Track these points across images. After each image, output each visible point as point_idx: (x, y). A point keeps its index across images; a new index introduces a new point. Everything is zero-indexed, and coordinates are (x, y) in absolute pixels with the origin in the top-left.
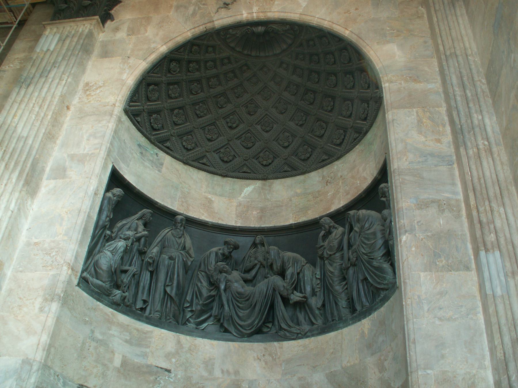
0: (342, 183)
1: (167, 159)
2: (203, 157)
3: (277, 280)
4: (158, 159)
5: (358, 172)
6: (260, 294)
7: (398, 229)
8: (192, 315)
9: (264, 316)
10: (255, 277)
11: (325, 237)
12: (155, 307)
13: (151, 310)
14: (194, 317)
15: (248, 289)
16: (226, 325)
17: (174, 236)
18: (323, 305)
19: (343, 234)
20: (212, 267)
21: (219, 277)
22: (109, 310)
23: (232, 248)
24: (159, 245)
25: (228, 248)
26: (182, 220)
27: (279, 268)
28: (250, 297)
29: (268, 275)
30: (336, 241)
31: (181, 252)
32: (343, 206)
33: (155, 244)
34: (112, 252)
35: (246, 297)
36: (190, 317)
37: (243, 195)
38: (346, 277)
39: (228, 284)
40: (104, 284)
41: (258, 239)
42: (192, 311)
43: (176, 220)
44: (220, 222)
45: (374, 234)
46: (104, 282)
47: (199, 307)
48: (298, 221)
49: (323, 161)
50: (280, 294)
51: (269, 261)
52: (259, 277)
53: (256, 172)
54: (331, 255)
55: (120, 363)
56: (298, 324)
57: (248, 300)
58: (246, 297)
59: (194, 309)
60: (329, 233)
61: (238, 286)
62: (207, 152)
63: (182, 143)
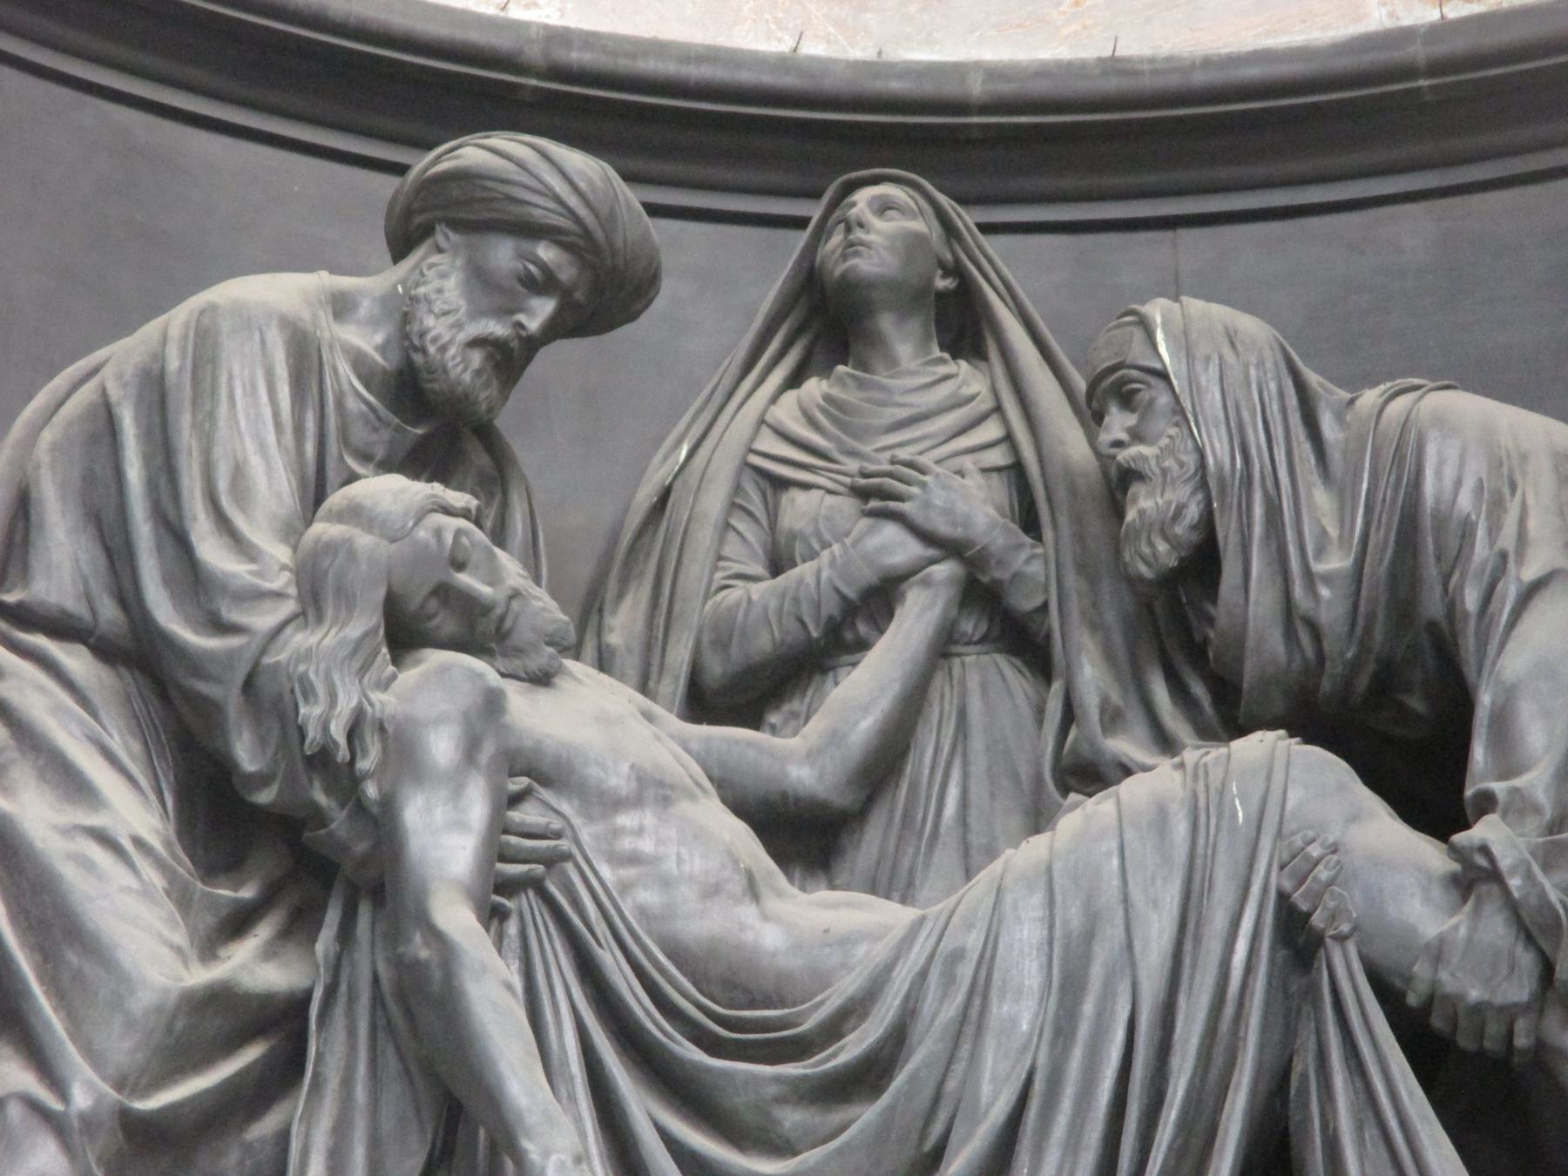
3: (1302, 787)
6: (1068, 987)
20: (254, 553)
21: (385, 702)
23: (543, 283)
25: (479, 277)
27: (1329, 606)
29: (1126, 745)
35: (834, 1030)
39: (528, 815)
51: (1144, 503)
52: (943, 783)
57: (868, 1077)
58: (834, 1030)
61: (680, 861)
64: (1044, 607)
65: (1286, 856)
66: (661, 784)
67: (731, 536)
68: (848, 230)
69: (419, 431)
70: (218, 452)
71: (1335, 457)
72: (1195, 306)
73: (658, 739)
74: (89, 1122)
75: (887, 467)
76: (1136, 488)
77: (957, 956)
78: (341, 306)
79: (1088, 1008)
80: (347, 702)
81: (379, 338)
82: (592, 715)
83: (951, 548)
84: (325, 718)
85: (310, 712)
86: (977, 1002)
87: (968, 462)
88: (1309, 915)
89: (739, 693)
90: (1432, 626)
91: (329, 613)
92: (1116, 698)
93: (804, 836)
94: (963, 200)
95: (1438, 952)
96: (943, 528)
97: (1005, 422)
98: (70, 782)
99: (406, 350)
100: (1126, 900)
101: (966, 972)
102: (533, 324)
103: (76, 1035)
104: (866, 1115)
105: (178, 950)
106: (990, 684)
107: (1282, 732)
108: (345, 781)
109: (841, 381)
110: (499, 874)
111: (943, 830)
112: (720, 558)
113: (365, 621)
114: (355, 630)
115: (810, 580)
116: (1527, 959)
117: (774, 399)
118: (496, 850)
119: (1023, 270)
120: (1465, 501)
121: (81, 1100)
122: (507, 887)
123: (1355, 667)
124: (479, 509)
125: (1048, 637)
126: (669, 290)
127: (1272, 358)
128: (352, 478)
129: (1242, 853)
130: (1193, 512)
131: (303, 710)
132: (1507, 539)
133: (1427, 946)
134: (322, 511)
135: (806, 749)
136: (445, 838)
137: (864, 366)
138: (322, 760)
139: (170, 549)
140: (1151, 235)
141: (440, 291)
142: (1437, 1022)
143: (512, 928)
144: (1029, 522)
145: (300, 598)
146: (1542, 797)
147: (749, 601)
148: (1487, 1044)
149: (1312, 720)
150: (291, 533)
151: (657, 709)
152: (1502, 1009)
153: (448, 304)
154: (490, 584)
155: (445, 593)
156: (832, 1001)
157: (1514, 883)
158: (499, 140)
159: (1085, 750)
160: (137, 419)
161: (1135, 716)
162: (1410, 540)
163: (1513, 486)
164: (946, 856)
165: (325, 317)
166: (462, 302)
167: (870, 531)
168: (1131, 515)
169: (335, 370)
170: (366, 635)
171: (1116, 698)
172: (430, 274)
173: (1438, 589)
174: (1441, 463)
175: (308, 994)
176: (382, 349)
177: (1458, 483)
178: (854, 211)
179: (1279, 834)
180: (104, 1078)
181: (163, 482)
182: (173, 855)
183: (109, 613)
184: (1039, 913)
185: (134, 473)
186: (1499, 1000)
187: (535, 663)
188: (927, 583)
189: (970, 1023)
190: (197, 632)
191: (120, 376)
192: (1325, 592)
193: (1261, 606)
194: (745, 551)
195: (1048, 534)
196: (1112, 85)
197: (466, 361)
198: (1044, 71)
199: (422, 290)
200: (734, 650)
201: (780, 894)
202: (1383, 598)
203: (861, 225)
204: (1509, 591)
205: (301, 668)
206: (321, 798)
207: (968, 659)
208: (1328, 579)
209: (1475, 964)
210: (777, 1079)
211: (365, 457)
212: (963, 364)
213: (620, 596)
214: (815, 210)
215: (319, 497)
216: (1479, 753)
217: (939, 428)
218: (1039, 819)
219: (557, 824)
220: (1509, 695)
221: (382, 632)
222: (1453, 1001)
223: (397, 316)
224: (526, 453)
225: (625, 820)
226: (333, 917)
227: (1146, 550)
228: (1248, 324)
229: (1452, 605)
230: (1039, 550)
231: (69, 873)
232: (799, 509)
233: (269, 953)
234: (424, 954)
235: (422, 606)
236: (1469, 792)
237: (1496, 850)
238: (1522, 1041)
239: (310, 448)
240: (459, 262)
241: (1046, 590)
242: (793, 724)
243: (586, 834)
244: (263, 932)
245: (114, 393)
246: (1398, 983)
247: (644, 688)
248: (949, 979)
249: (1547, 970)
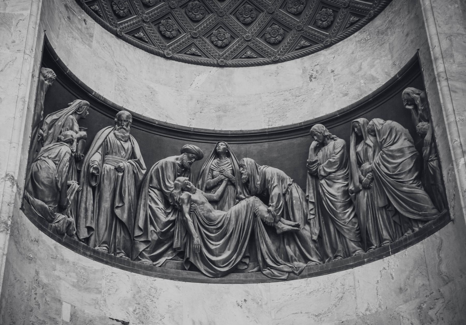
0: (335, 80)
1: (97, 29)
2: (138, 30)
4: (87, 28)
5: (360, 69)
7: (451, 148)
8: (147, 248)
9: (244, 250)
11: (317, 149)
12: (101, 236)
13: (95, 241)
14: (148, 249)
15: (217, 214)
16: (192, 260)
17: (119, 139)
18: (320, 237)
19: (347, 147)
20: (170, 183)
21: (181, 197)
22: (51, 242)
23: (194, 158)
24: (100, 151)
26: (128, 117)
27: (258, 186)
30: (338, 156)
31: (130, 161)
32: (338, 111)
33: (95, 148)
34: (54, 160)
36: (144, 250)
37: (194, 86)
38: (355, 203)
39: (193, 206)
40: (46, 206)
41: (222, 146)
42: (147, 242)
43: (120, 116)
44: (169, 121)
45: (401, 150)
46: (46, 203)
47: (155, 237)
48: (274, 126)
49: (302, 47)
50: (262, 221)
51: (244, 176)
53: (209, 55)
54: (330, 173)
55: (69, 316)
56: (287, 259)
59: (150, 239)
60: (322, 144)
62: (144, 21)
63: (112, 7)
72: (248, 159)
74: (159, 233)
80: (178, 196)
82: (199, 196)
83: (227, 177)
87: (229, 169)
89: (209, 189)
95: (266, 218)
98: (156, 203)
101: (228, 219)
102: (193, 161)
103: (157, 225)
106: (231, 189)
108: (178, 203)
116: (273, 219)
118: (190, 209)
119: (233, 148)
120: (269, 179)
122: (191, 211)
132: (273, 182)
135: (215, 195)
136: (186, 209)
138: (177, 201)
144: (234, 175)
150: (174, 181)
155: (187, 187)
162: (265, 181)
183: (159, 187)
185: (161, 176)
189: (229, 223)
193: (253, 186)
198: (235, 131)
204: (272, 187)
209: (270, 220)
216: (270, 201)
217: (227, 165)
220: (273, 196)
222: (267, 222)
225: (201, 206)
229: (268, 187)
231: (156, 211)
232: (215, 173)
244: (172, 214)
247: (202, 190)
249: (275, 220)
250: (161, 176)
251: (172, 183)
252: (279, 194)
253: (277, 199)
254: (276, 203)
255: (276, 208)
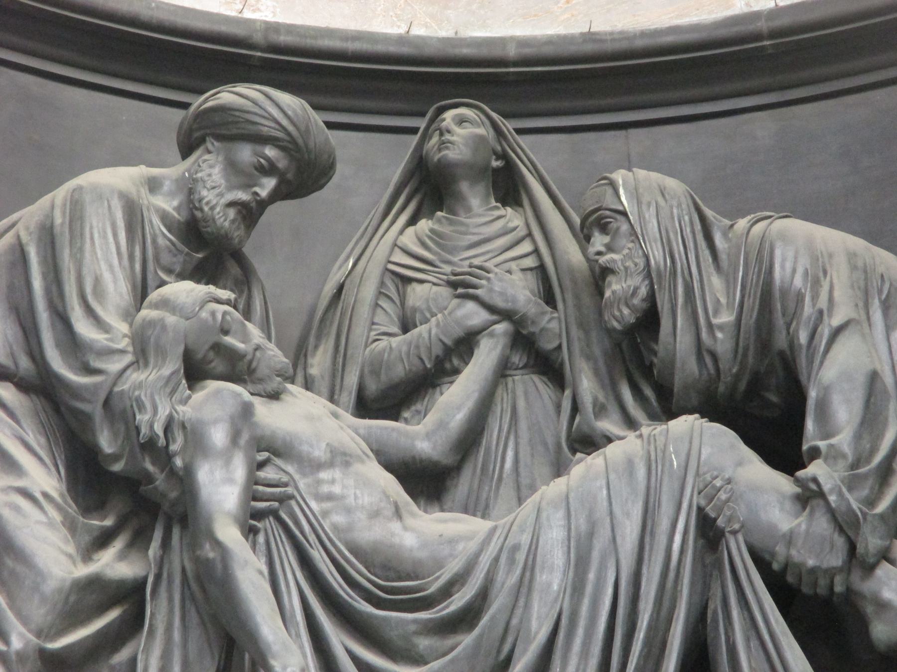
6: (580, 564)
10: (470, 440)
20: (107, 327)
21: (185, 411)
23: (268, 169)
25: (232, 166)
27: (722, 343)
28: (483, 596)
29: (608, 425)
35: (447, 592)
39: (269, 473)
50: (761, 562)
51: (615, 287)
52: (504, 449)
57: (466, 619)
58: (447, 592)
61: (356, 498)
64: (559, 347)
65: (701, 486)
66: (345, 454)
67: (379, 311)
68: (441, 134)
69: (200, 256)
70: (85, 271)
71: (723, 257)
72: (641, 173)
73: (342, 428)
74: (21, 656)
75: (469, 270)
76: (610, 278)
77: (516, 548)
78: (153, 185)
79: (591, 576)
80: (163, 412)
81: (175, 203)
82: (304, 416)
83: (506, 315)
84: (152, 420)
85: (142, 418)
86: (528, 574)
87: (513, 265)
88: (715, 520)
90: (781, 354)
91: (152, 360)
92: (601, 398)
93: (426, 481)
94: (506, 116)
95: (789, 539)
96: (500, 303)
97: (534, 241)
99: (191, 209)
100: (611, 513)
101: (521, 557)
102: (264, 193)
104: (467, 640)
105: (70, 556)
106: (529, 391)
107: (697, 415)
108: (164, 457)
109: (439, 221)
110: (253, 508)
111: (505, 476)
112: (373, 324)
113: (173, 365)
114: (166, 371)
115: (426, 335)
116: (840, 541)
117: (401, 232)
118: (251, 494)
119: (542, 154)
120: (798, 282)
121: (17, 644)
122: (258, 515)
123: (737, 377)
124: (236, 300)
125: (562, 364)
126: (341, 170)
127: (686, 203)
128: (162, 283)
129: (677, 485)
130: (643, 291)
131: (138, 417)
132: (823, 303)
133: (784, 535)
134: (145, 303)
135: (426, 431)
136: (221, 489)
137: (452, 212)
138: (149, 446)
139: (60, 326)
140: (612, 133)
141: (210, 175)
142: (790, 579)
143: (261, 538)
144: (549, 299)
145: (135, 353)
146: (847, 449)
147: (391, 348)
148: (819, 591)
149: (714, 409)
150: (128, 316)
151: (340, 411)
152: (826, 571)
153: (215, 181)
154: (243, 342)
155: (217, 348)
156: (445, 576)
157: (832, 498)
158: (242, 88)
159: (585, 429)
160: (38, 253)
161: (613, 408)
162: (767, 305)
163: (825, 273)
164: (507, 491)
165: (144, 191)
166: (223, 181)
167: (459, 306)
168: (608, 294)
169: (151, 222)
170: (173, 374)
171: (601, 398)
172: (204, 166)
173: (784, 332)
174: (784, 260)
175: (144, 580)
176: (178, 209)
177: (794, 271)
178: (444, 123)
179: (697, 474)
180: (29, 631)
181: (54, 289)
182: (65, 502)
183: (25, 364)
184: (562, 523)
185: (37, 284)
186: (825, 565)
187: (271, 386)
188: (492, 335)
189: (524, 587)
190: (76, 374)
191: (27, 228)
192: (719, 335)
193: (684, 343)
194: (388, 321)
195: (560, 305)
196: (589, 48)
197: (225, 215)
198: (550, 41)
199: (199, 175)
200: (383, 377)
201: (413, 515)
202: (753, 338)
203: (449, 132)
204: (825, 332)
205: (137, 393)
206: (150, 467)
207: (516, 378)
208: (721, 328)
209: (811, 545)
210: (415, 621)
211: (169, 271)
212: (509, 209)
213: (316, 347)
214: (422, 123)
215: (144, 294)
216: (810, 425)
218: (559, 469)
219: (285, 479)
221: (182, 371)
222: (799, 566)
223: (186, 190)
224: (261, 266)
225: (324, 475)
226: (158, 535)
227: (617, 313)
228: (672, 183)
230: (556, 315)
232: (417, 294)
233: (122, 556)
234: (211, 555)
235: (205, 356)
236: (805, 447)
237: (821, 480)
238: (839, 588)
239: (138, 267)
240: (220, 158)
241: (560, 336)
242: (417, 417)
243: (302, 484)
244: (118, 545)
245: (25, 238)
246: (767, 557)
247: (332, 399)
248: (512, 561)
250: (37, 284)
251: (123, 328)
252: (874, 377)
253: (858, 406)
254: (858, 437)
255: (855, 466)
